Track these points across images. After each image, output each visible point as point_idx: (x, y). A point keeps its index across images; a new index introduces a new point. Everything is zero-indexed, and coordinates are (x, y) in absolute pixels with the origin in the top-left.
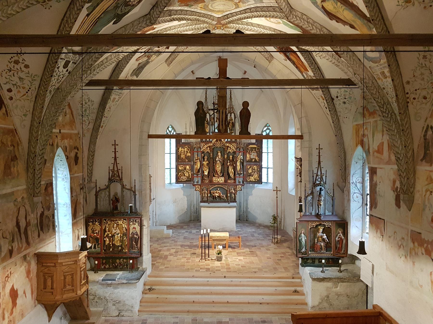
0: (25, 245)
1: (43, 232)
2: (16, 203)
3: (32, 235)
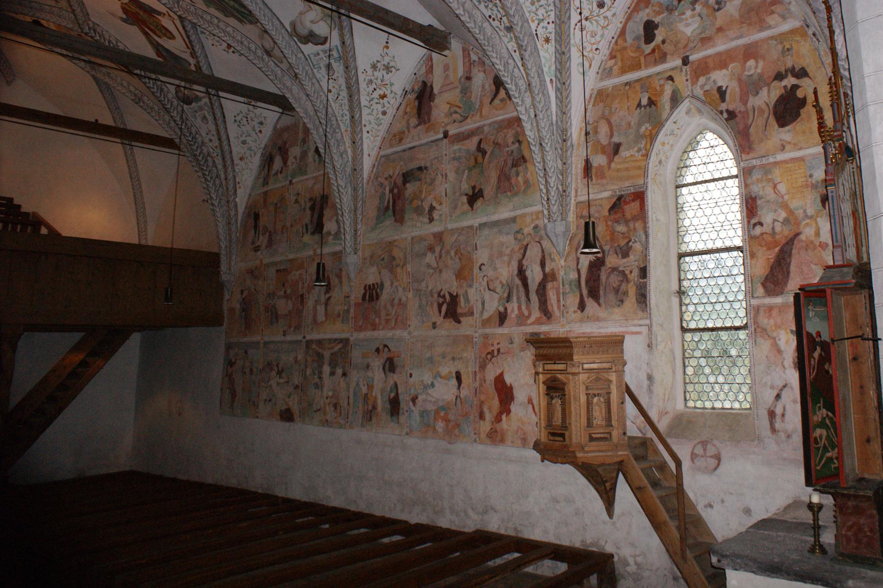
0: (536, 314)
1: (599, 304)
2: (519, 236)
3: (559, 301)
